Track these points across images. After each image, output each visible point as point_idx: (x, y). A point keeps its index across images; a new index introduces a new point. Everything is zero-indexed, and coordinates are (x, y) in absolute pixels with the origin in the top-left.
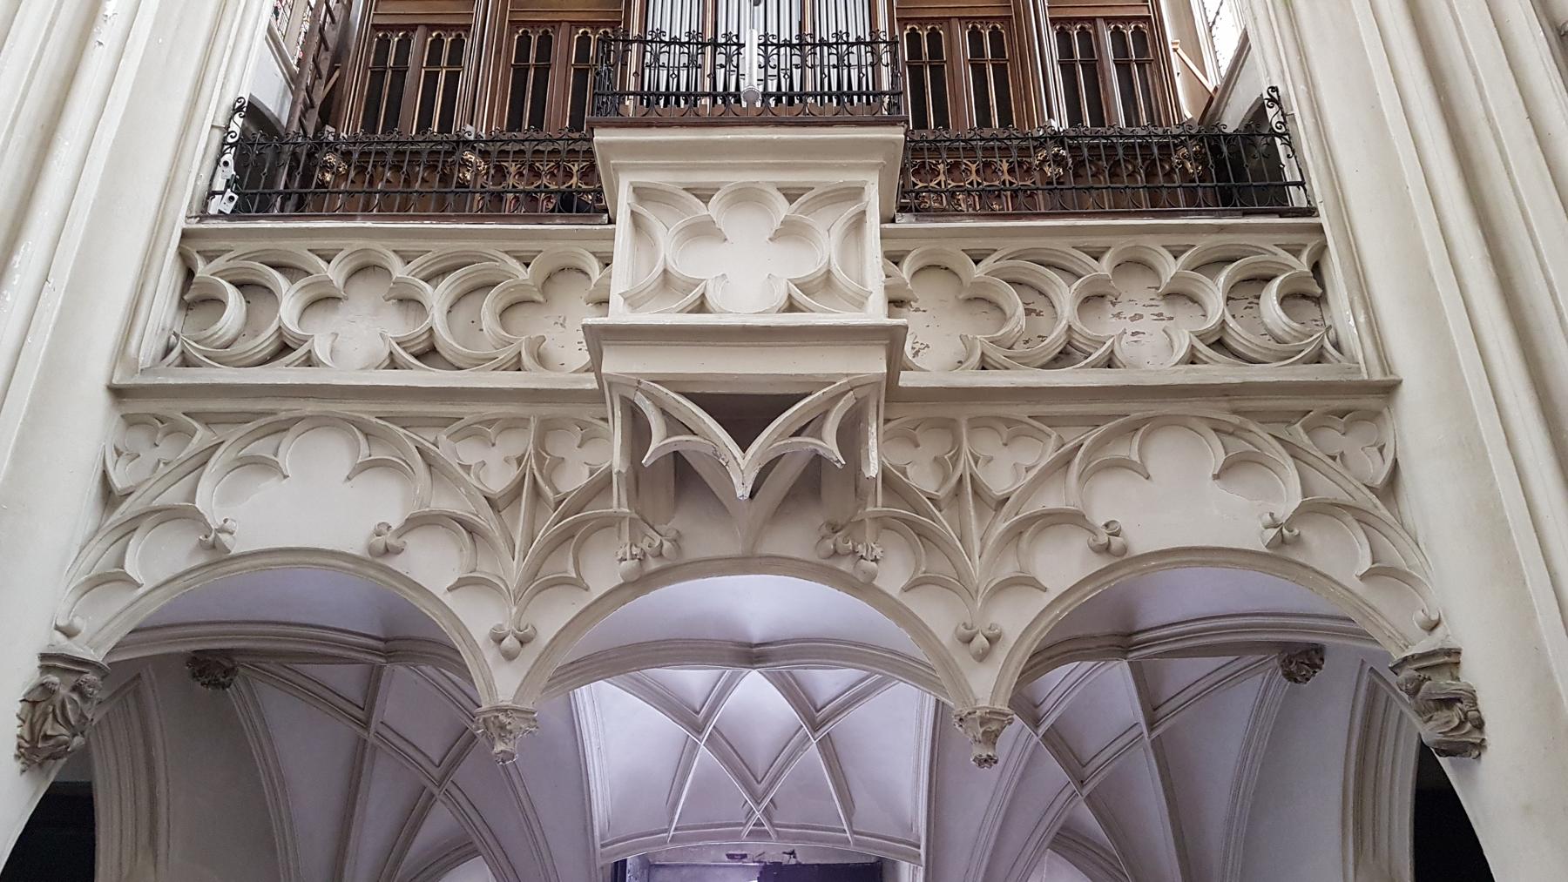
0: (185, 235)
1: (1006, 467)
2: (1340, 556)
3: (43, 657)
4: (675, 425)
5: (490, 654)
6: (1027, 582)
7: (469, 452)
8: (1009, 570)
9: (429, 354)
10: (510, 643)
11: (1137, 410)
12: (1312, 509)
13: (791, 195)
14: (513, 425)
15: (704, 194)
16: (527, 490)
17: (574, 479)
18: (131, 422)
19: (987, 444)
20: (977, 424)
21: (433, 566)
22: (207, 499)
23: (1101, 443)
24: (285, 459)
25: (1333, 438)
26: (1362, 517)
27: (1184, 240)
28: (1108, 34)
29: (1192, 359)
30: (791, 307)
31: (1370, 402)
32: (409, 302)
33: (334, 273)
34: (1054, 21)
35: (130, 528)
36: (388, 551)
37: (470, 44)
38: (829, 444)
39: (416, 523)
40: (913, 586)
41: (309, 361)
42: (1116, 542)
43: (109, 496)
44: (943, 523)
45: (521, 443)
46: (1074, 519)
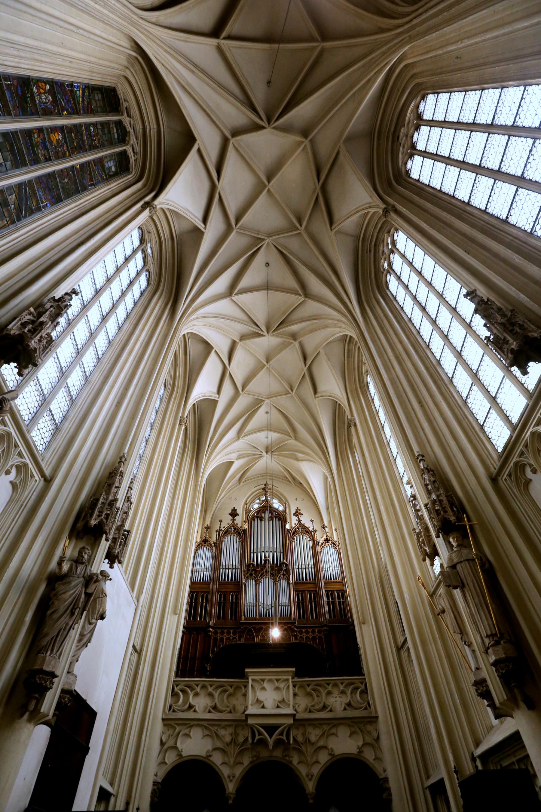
0: (174, 681)
1: (314, 734)
2: (369, 755)
3: (154, 782)
4: (260, 733)
5: (228, 780)
6: (317, 762)
7: (222, 732)
8: (314, 759)
10: (231, 778)
11: (336, 722)
12: (365, 744)
14: (230, 726)
15: (263, 680)
16: (234, 741)
17: (241, 739)
18: (165, 725)
19: (310, 729)
20: (309, 725)
21: (217, 759)
22: (179, 745)
23: (330, 729)
25: (369, 727)
26: (373, 746)
27: (343, 681)
28: (336, 594)
29: (345, 709)
30: (278, 707)
31: (374, 720)
32: (211, 695)
34: (325, 591)
35: (166, 751)
36: (210, 756)
37: (210, 597)
38: (284, 738)
39: (215, 749)
40: (299, 763)
42: (333, 753)
43: (162, 744)
44: (303, 748)
45: (231, 730)
46: (325, 747)
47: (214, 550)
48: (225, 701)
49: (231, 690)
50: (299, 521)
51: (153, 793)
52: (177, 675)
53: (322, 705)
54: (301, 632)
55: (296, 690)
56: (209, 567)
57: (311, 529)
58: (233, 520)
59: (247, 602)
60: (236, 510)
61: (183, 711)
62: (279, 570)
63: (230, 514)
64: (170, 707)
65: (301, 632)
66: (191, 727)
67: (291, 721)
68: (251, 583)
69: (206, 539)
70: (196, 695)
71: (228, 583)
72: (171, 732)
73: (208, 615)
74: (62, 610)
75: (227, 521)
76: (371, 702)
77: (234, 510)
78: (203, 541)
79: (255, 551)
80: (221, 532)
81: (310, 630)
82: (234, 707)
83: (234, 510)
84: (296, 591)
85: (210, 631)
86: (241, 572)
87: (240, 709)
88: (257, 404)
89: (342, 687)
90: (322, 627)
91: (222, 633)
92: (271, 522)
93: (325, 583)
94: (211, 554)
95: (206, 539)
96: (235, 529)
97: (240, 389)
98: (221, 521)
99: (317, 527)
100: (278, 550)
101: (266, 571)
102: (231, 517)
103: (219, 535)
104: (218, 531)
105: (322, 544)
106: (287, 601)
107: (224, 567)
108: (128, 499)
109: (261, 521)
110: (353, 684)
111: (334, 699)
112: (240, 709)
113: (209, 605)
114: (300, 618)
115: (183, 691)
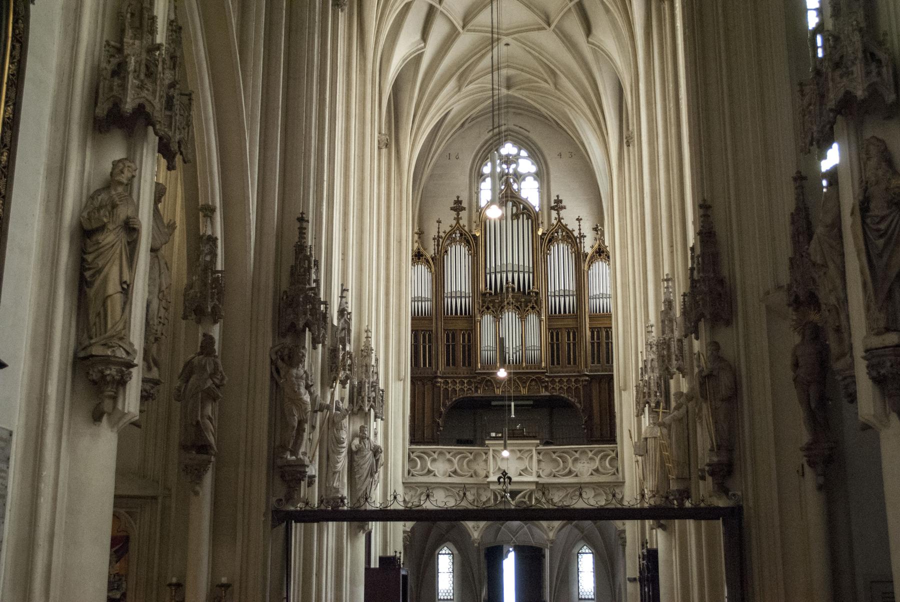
9: (455, 472)
13: (520, 451)
18: (405, 487)
29: (592, 474)
30: (520, 475)
32: (449, 461)
33: (436, 456)
37: (433, 336)
45: (474, 491)
47: (433, 269)
48: (465, 467)
49: (471, 457)
50: (559, 219)
51: (405, 539)
52: (412, 442)
53: (567, 470)
56: (426, 291)
57: (576, 234)
58: (458, 219)
60: (461, 202)
63: (452, 209)
64: (409, 472)
65: (553, 382)
66: (433, 488)
67: (534, 487)
69: (419, 252)
70: (434, 460)
71: (456, 318)
72: (412, 493)
73: (433, 362)
74: (365, 475)
75: (449, 220)
76: (620, 469)
77: (458, 202)
78: (416, 256)
79: (493, 270)
82: (475, 473)
83: (458, 202)
84: (549, 329)
86: (473, 301)
87: (484, 473)
89: (590, 455)
92: (515, 222)
94: (430, 275)
95: (419, 252)
96: (461, 235)
99: (587, 228)
100: (526, 270)
102: (454, 214)
103: (438, 245)
105: (592, 257)
106: (537, 344)
107: (449, 295)
111: (582, 465)
113: (433, 348)
114: (553, 363)
115: (419, 457)
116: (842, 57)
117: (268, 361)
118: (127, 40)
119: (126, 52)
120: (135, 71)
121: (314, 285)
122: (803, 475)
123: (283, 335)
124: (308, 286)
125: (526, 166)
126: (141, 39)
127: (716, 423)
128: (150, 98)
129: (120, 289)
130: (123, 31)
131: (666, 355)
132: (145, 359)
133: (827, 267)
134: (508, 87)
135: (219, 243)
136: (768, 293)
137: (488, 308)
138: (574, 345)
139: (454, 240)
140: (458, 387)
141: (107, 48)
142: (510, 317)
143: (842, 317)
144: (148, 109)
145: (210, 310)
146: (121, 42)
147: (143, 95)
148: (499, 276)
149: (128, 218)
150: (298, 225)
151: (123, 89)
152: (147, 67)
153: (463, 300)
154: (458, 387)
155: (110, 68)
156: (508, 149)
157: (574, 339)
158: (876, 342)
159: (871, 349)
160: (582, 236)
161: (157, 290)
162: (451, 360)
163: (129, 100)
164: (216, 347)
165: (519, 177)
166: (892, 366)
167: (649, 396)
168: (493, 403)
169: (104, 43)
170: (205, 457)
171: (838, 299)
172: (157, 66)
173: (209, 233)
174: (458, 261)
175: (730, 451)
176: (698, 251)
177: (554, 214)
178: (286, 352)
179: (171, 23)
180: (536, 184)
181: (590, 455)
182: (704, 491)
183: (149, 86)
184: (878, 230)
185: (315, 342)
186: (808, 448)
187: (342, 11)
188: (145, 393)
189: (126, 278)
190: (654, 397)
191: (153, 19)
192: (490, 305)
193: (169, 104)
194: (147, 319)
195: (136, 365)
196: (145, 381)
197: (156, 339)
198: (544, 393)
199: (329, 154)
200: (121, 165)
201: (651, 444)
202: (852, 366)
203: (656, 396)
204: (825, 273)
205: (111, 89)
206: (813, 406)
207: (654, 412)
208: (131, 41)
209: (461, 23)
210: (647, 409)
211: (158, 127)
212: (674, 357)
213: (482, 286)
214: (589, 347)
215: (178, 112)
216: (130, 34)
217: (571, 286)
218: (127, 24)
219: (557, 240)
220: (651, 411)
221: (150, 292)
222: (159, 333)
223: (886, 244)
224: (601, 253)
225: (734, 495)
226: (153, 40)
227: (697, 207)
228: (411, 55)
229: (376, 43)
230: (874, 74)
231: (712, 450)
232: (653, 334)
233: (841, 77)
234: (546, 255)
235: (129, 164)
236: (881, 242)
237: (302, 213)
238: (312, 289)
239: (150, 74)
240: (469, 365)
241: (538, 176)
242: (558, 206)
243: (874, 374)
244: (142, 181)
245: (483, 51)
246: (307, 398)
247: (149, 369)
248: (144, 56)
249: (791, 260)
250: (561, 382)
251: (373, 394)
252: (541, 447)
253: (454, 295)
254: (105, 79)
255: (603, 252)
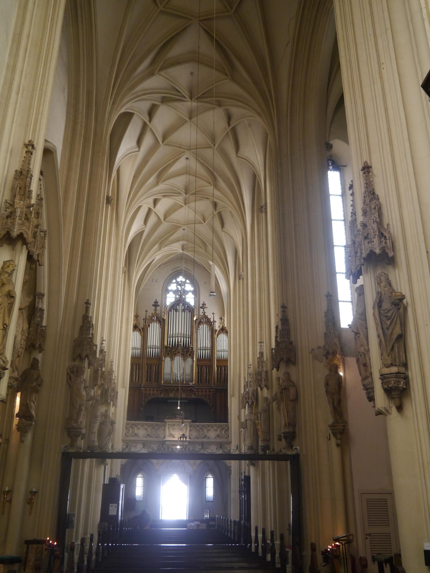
7: (153, 446)
9: (148, 435)
24: (137, 446)
29: (216, 438)
32: (146, 429)
41: (138, 436)
49: (157, 428)
53: (204, 435)
54: (198, 391)
55: (191, 428)
56: (139, 345)
57: (212, 320)
58: (156, 310)
59: (165, 372)
60: (157, 302)
61: (131, 436)
62: (186, 351)
63: (153, 305)
65: (198, 391)
67: (187, 443)
68: (168, 359)
69: (136, 325)
70: (138, 429)
75: (151, 310)
77: (156, 302)
80: (147, 320)
81: (204, 390)
83: (156, 302)
85: (142, 390)
87: (162, 436)
88: (176, 228)
89: (215, 428)
90: (212, 389)
91: (150, 390)
93: (217, 361)
94: (141, 337)
95: (136, 325)
97: (160, 141)
98: (146, 311)
99: (217, 319)
100: (187, 336)
101: (178, 352)
102: (154, 308)
104: (145, 319)
105: (219, 331)
107: (149, 347)
108: (102, 351)
109: (176, 311)
110: (222, 426)
112: (162, 436)
113: (140, 372)
114: (198, 382)
116: (368, 234)
117: (66, 373)
118: (17, 200)
119: (15, 206)
120: (19, 216)
121: (91, 336)
122: (330, 439)
123: (74, 360)
124: (88, 337)
125: (189, 287)
126: (24, 201)
127: (287, 412)
128: (27, 230)
129: (2, 328)
130: (15, 196)
131: (260, 378)
132: (11, 366)
133: (359, 334)
134: (183, 250)
135: (45, 312)
136: (313, 350)
137: (168, 354)
138: (209, 373)
139: (153, 321)
140: (151, 392)
141: (5, 204)
142: (178, 359)
143: (367, 359)
144: (25, 236)
145: (38, 346)
146: (14, 202)
147: (23, 228)
148: (174, 339)
149: (9, 291)
150: (85, 306)
151: (13, 225)
152: (26, 215)
153: (156, 350)
154: (151, 392)
155: (6, 214)
156: (181, 279)
157: (209, 371)
158: (386, 371)
159: (383, 375)
160: (214, 322)
161: (21, 330)
162: (149, 379)
163: (15, 230)
164: (40, 365)
165: (185, 292)
166: (394, 383)
167: (249, 399)
168: (169, 401)
169: (4, 201)
170: (30, 422)
171: (365, 350)
172: (31, 215)
173: (40, 307)
174: (154, 330)
175: (294, 426)
176: (280, 327)
177: (201, 310)
178: (75, 369)
179: (38, 196)
180: (193, 296)
181: (215, 428)
182: (279, 446)
183: (27, 224)
184: (387, 316)
185: (89, 364)
186: (332, 427)
187: (110, 205)
188: (10, 385)
189: (7, 322)
190: (251, 400)
191: (30, 192)
192: (169, 353)
193: (35, 236)
194: (14, 345)
195: (7, 369)
196: (10, 378)
197: (18, 356)
198: (193, 396)
199: (100, 273)
200: (8, 263)
201: (249, 423)
202: (372, 382)
203: (252, 399)
204: (359, 337)
205: (6, 224)
206: (335, 405)
207: (250, 406)
208: (18, 201)
209: (163, 218)
210: (247, 406)
211: (29, 246)
212: (263, 380)
213: (166, 343)
214: (216, 375)
215: (38, 240)
216: (18, 198)
217: (209, 345)
218: (17, 193)
219: (203, 323)
220: (250, 406)
221: (17, 331)
222: (20, 353)
223: (391, 323)
224: (223, 330)
225: (295, 448)
226: (30, 202)
227: (280, 307)
228: (139, 231)
229: (124, 223)
230: (384, 242)
231: (285, 425)
232: (251, 369)
233: (369, 243)
234: (197, 329)
235: (13, 263)
236: (389, 322)
237: (88, 300)
238: (90, 338)
239: (27, 219)
240: (158, 381)
241: (194, 292)
242: (203, 306)
243: (386, 387)
244: (18, 273)
245: (173, 232)
246: (84, 393)
247: (13, 371)
248: (25, 209)
249: (325, 334)
250: (202, 391)
251: (113, 394)
252: (192, 424)
253: (152, 347)
254: (3, 219)
255: (224, 329)
